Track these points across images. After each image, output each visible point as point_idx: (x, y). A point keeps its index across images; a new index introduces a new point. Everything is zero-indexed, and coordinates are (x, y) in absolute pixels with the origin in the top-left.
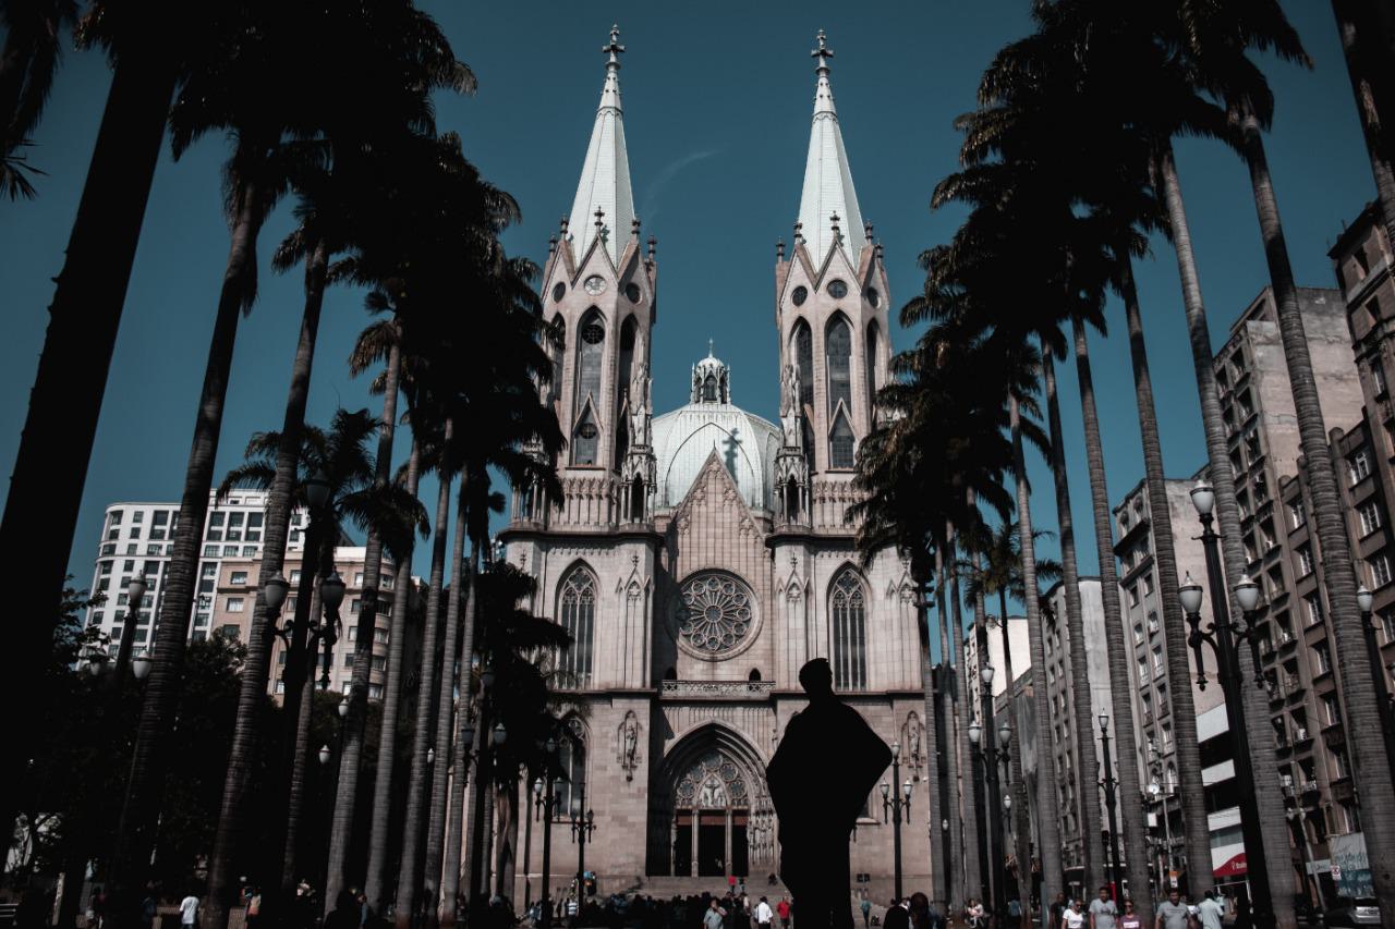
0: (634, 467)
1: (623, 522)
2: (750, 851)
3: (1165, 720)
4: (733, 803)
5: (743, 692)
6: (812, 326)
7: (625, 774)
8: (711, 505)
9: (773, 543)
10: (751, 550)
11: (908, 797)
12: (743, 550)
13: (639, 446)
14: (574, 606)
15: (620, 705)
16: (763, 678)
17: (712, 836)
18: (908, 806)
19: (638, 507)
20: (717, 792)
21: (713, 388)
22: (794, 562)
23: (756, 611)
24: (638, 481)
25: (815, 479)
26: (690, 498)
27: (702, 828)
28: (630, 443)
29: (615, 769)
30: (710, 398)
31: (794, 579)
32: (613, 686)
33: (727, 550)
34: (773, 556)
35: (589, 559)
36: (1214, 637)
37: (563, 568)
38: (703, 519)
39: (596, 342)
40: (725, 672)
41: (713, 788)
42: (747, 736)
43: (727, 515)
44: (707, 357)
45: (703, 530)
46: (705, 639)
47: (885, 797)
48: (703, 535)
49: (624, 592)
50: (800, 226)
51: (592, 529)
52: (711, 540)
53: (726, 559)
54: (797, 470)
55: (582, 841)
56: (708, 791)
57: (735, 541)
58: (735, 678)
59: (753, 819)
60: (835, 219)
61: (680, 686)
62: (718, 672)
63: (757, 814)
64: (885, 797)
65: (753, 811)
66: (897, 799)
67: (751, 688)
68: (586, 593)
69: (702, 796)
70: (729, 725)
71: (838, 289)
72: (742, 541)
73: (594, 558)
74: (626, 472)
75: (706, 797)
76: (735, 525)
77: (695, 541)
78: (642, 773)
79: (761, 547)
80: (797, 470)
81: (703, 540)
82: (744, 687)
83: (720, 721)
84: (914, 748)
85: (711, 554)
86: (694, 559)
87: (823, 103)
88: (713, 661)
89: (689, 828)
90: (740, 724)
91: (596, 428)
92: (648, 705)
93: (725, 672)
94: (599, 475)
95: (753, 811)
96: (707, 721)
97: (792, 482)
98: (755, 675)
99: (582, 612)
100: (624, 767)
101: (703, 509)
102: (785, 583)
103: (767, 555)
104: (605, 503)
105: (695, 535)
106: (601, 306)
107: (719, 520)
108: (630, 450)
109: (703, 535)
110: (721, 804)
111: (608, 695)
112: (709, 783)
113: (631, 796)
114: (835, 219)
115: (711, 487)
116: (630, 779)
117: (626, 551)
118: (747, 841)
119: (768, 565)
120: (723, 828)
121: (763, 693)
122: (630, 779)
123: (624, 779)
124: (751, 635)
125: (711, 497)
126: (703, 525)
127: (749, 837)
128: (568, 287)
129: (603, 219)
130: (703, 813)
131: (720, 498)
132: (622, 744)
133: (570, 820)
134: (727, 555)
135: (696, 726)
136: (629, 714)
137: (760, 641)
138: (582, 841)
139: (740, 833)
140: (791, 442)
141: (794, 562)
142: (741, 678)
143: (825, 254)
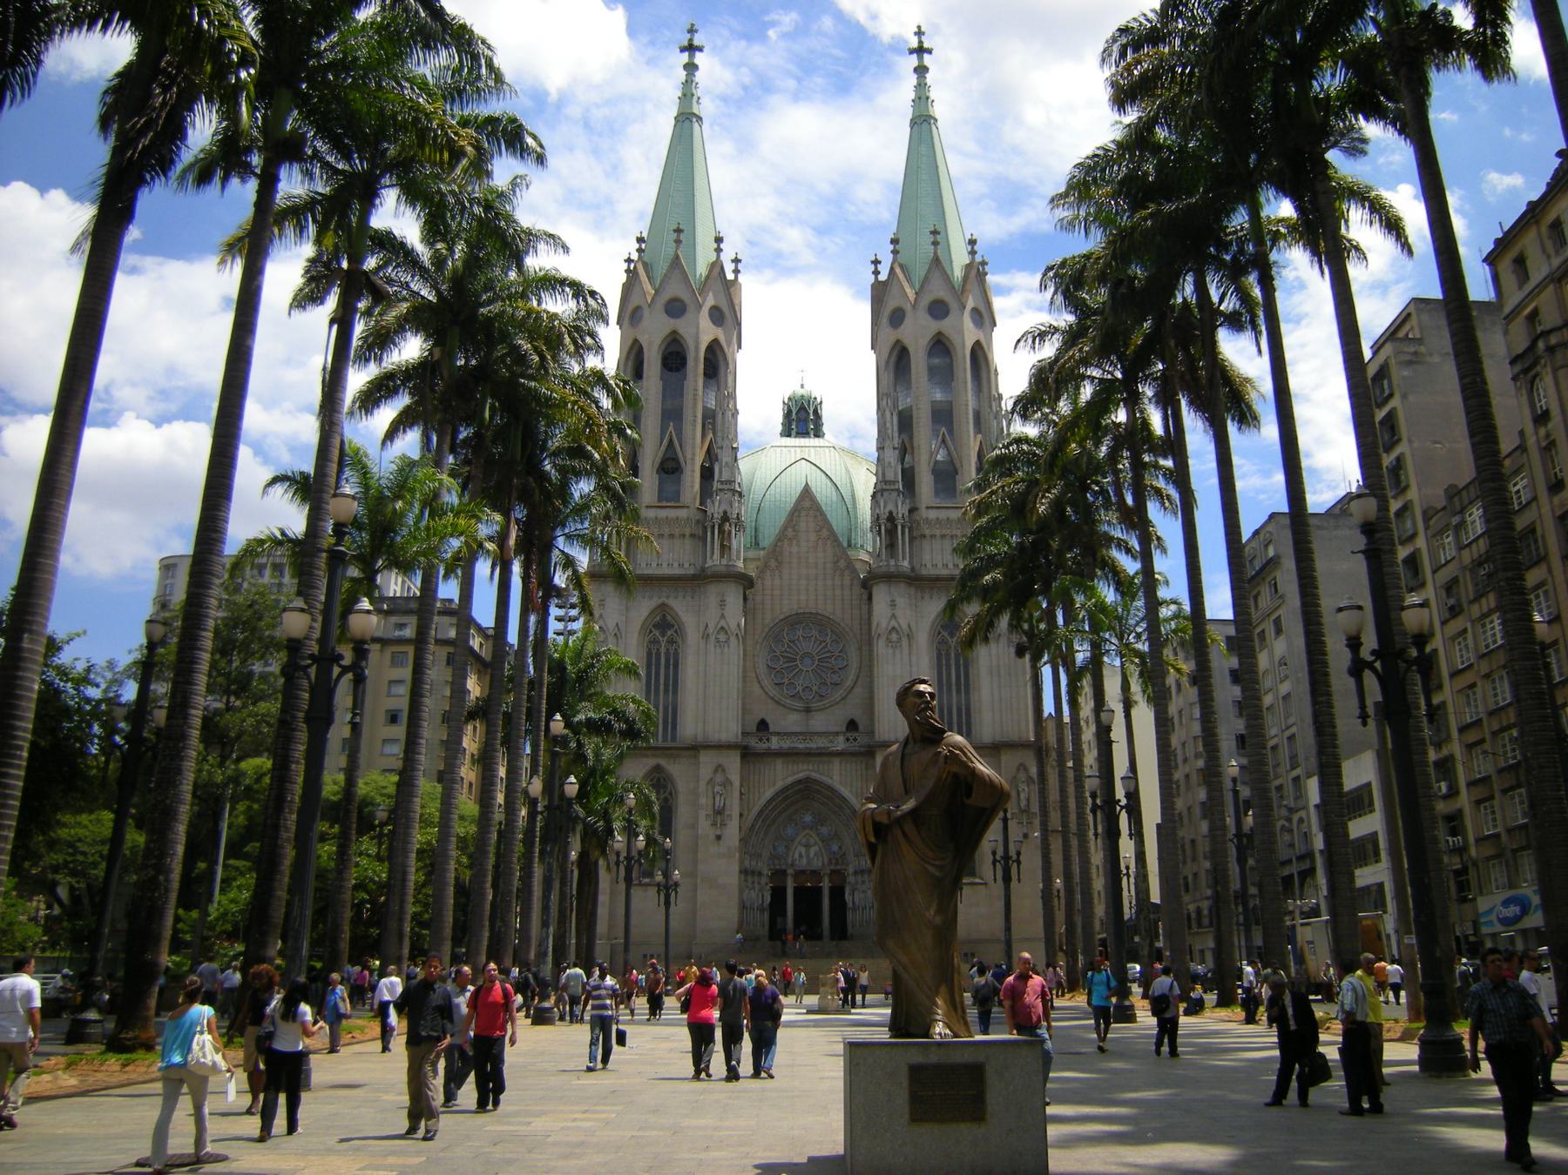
1: (709, 563)
2: (850, 915)
3: (1294, 773)
4: (830, 863)
5: (840, 744)
6: (911, 350)
7: (712, 833)
9: (867, 585)
10: (847, 592)
11: (1018, 854)
12: (838, 592)
13: (726, 482)
14: (658, 654)
15: (707, 760)
16: (861, 728)
17: (808, 897)
18: (1019, 862)
19: (725, 548)
20: (813, 851)
21: (806, 420)
22: (893, 605)
23: (853, 656)
24: (725, 518)
26: (781, 537)
27: (796, 889)
29: (704, 826)
31: (893, 623)
32: (700, 739)
34: (870, 598)
35: (672, 602)
36: (1378, 665)
37: (645, 613)
39: (678, 370)
40: (819, 722)
41: (807, 846)
42: (845, 792)
46: (799, 688)
47: (994, 853)
49: (712, 638)
51: (677, 571)
52: (804, 582)
55: (667, 904)
56: (803, 850)
57: (829, 583)
58: (831, 729)
59: (851, 879)
60: (935, 233)
61: (774, 740)
62: (812, 722)
63: (856, 873)
64: (994, 853)
65: (851, 870)
66: (1006, 857)
68: (671, 642)
70: (824, 779)
71: (938, 309)
72: (838, 582)
73: (681, 606)
74: (715, 509)
76: (829, 566)
78: (732, 831)
79: (857, 589)
82: (841, 738)
83: (815, 775)
84: (1023, 803)
85: (803, 597)
88: (808, 710)
89: (784, 889)
90: (836, 778)
91: (678, 462)
92: (738, 759)
93: (819, 722)
94: (683, 513)
95: (851, 870)
96: (801, 775)
97: (891, 518)
98: (852, 725)
99: (667, 660)
100: (714, 824)
101: (795, 549)
102: (884, 625)
103: (865, 597)
104: (688, 541)
106: (681, 331)
110: (817, 864)
111: (695, 749)
115: (803, 525)
116: (719, 838)
117: (713, 591)
119: (865, 608)
121: (863, 740)
122: (719, 838)
123: (712, 837)
124: (849, 683)
127: (848, 897)
128: (646, 312)
129: (682, 237)
131: (813, 537)
132: (710, 802)
135: (790, 780)
136: (719, 768)
137: (858, 690)
138: (667, 904)
139: (837, 893)
140: (890, 476)
141: (893, 605)
142: (837, 729)
143: (923, 274)
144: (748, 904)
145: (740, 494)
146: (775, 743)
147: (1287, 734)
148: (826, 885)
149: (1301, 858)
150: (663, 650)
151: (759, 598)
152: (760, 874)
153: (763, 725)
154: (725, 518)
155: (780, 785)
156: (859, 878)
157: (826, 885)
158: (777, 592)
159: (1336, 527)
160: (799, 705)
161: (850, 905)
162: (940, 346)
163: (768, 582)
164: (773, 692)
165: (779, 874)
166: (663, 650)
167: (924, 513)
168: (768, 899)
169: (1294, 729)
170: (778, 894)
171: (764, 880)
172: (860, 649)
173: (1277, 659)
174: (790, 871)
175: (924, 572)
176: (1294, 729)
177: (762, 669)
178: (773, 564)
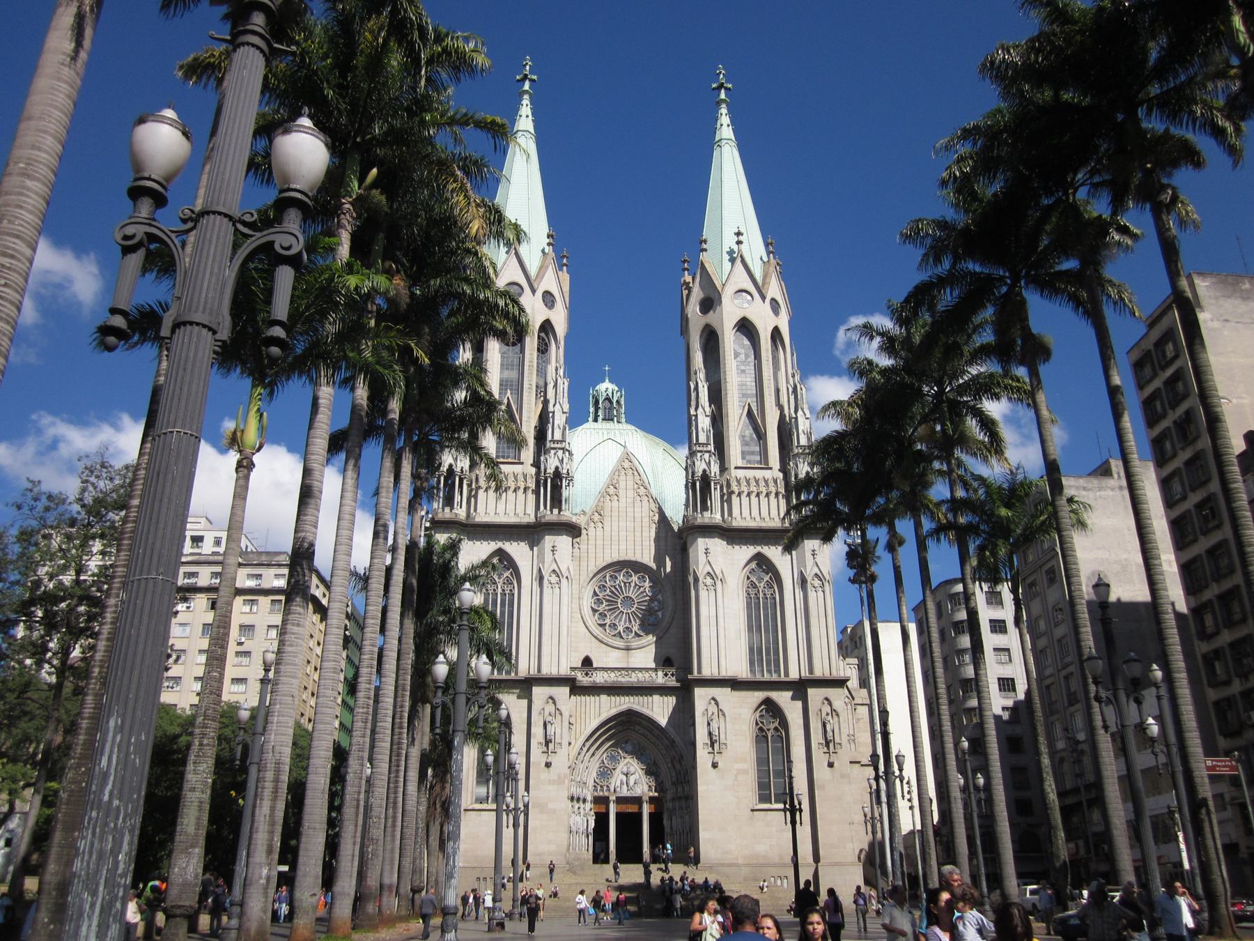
0: (551, 463)
7: (544, 759)
8: (622, 500)
13: (558, 442)
17: (629, 823)
19: (557, 501)
20: (632, 779)
21: (611, 409)
24: (557, 474)
25: (726, 476)
26: (605, 494)
27: (618, 815)
28: (549, 437)
30: (609, 418)
33: (638, 543)
38: (615, 514)
43: (637, 509)
44: (604, 381)
45: (615, 524)
46: (621, 628)
48: (615, 528)
50: (705, 241)
53: (638, 552)
54: (706, 463)
59: (670, 805)
60: (739, 234)
62: (631, 660)
63: (673, 799)
67: (666, 675)
69: (618, 783)
75: (622, 783)
77: (607, 533)
80: (706, 463)
81: (615, 534)
85: (623, 547)
86: (607, 551)
87: (725, 131)
89: (607, 814)
96: (624, 707)
101: (615, 504)
105: (607, 528)
107: (630, 515)
108: (548, 445)
109: (615, 528)
112: (625, 770)
113: (551, 782)
114: (739, 234)
115: (622, 484)
116: (548, 765)
118: (663, 827)
120: (640, 815)
122: (548, 765)
125: (622, 493)
126: (615, 519)
127: (666, 822)
130: (620, 800)
131: (631, 493)
133: (494, 806)
134: (638, 548)
135: (614, 712)
144: (574, 829)
145: (571, 454)
146: (599, 678)
147: (1064, 673)
148: (646, 809)
149: (1088, 787)
150: (500, 591)
151: (583, 547)
152: (585, 801)
153: (587, 662)
154: (557, 474)
155: (605, 715)
156: (677, 804)
157: (646, 809)
158: (599, 542)
159: (1100, 489)
160: (621, 644)
161: (667, 830)
162: (746, 327)
163: (591, 531)
164: (598, 631)
165: (601, 801)
166: (500, 591)
167: (736, 473)
168: (592, 824)
169: (1071, 669)
170: (602, 820)
171: (589, 805)
172: (674, 594)
173: (1050, 608)
174: (613, 798)
175: (735, 524)
176: (1071, 669)
177: (587, 612)
178: (596, 517)
